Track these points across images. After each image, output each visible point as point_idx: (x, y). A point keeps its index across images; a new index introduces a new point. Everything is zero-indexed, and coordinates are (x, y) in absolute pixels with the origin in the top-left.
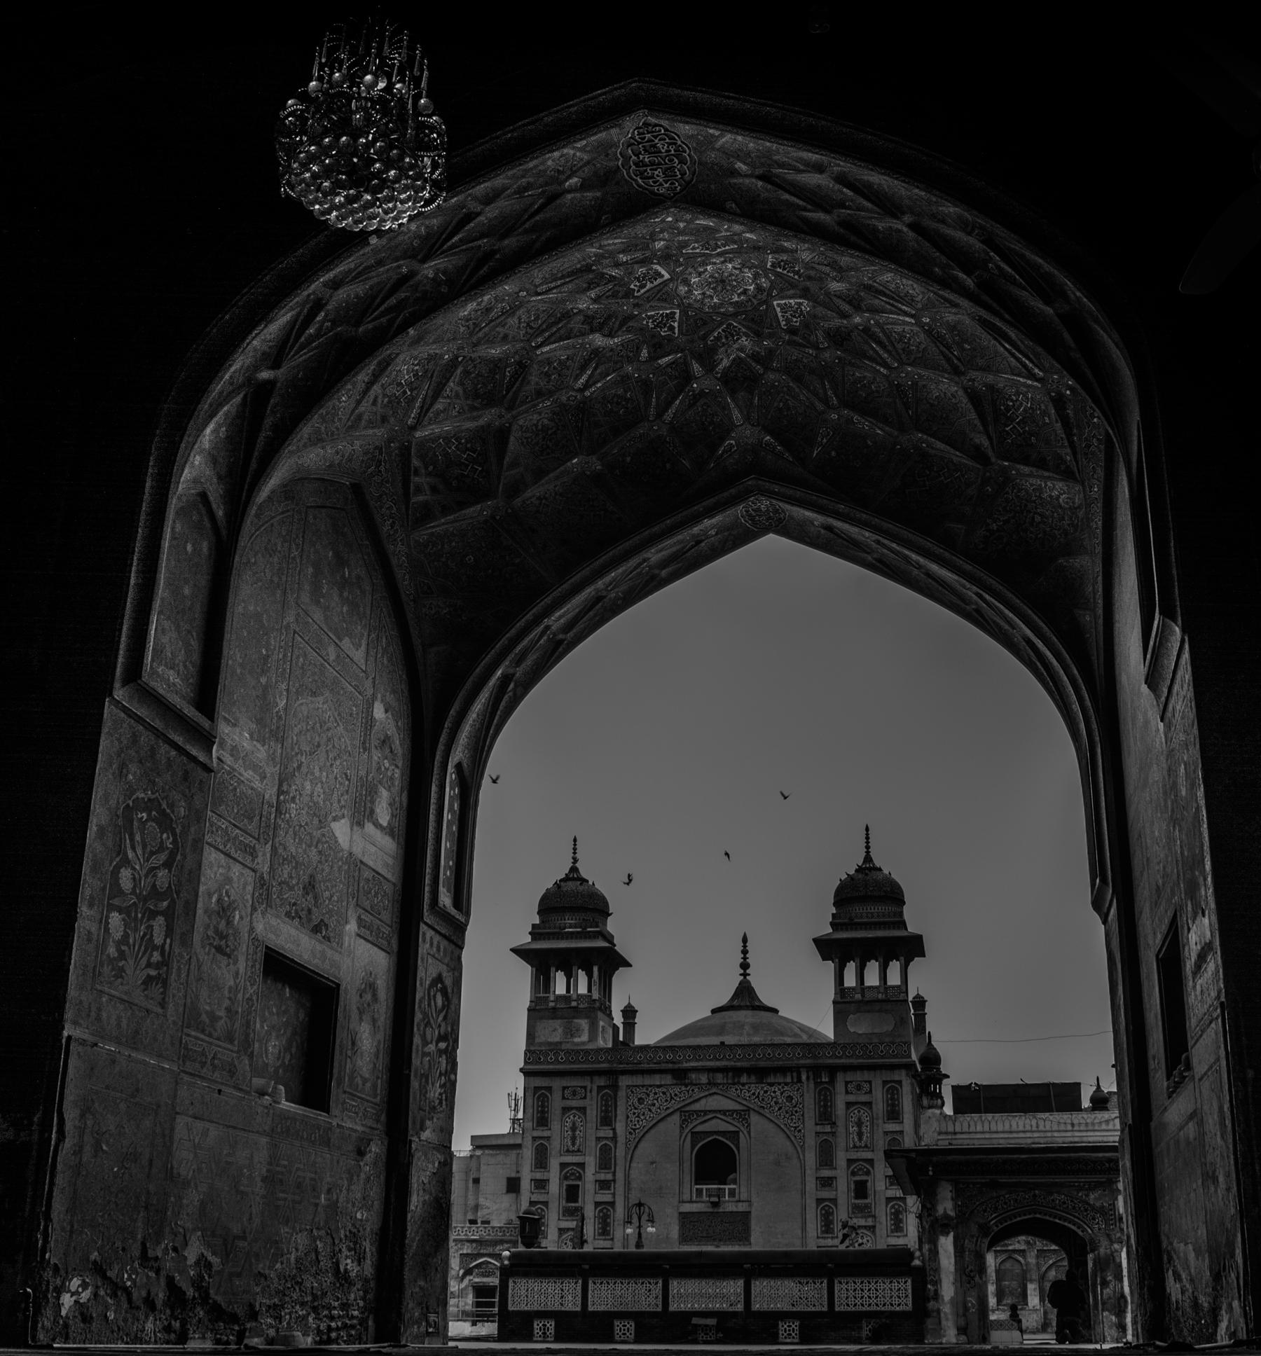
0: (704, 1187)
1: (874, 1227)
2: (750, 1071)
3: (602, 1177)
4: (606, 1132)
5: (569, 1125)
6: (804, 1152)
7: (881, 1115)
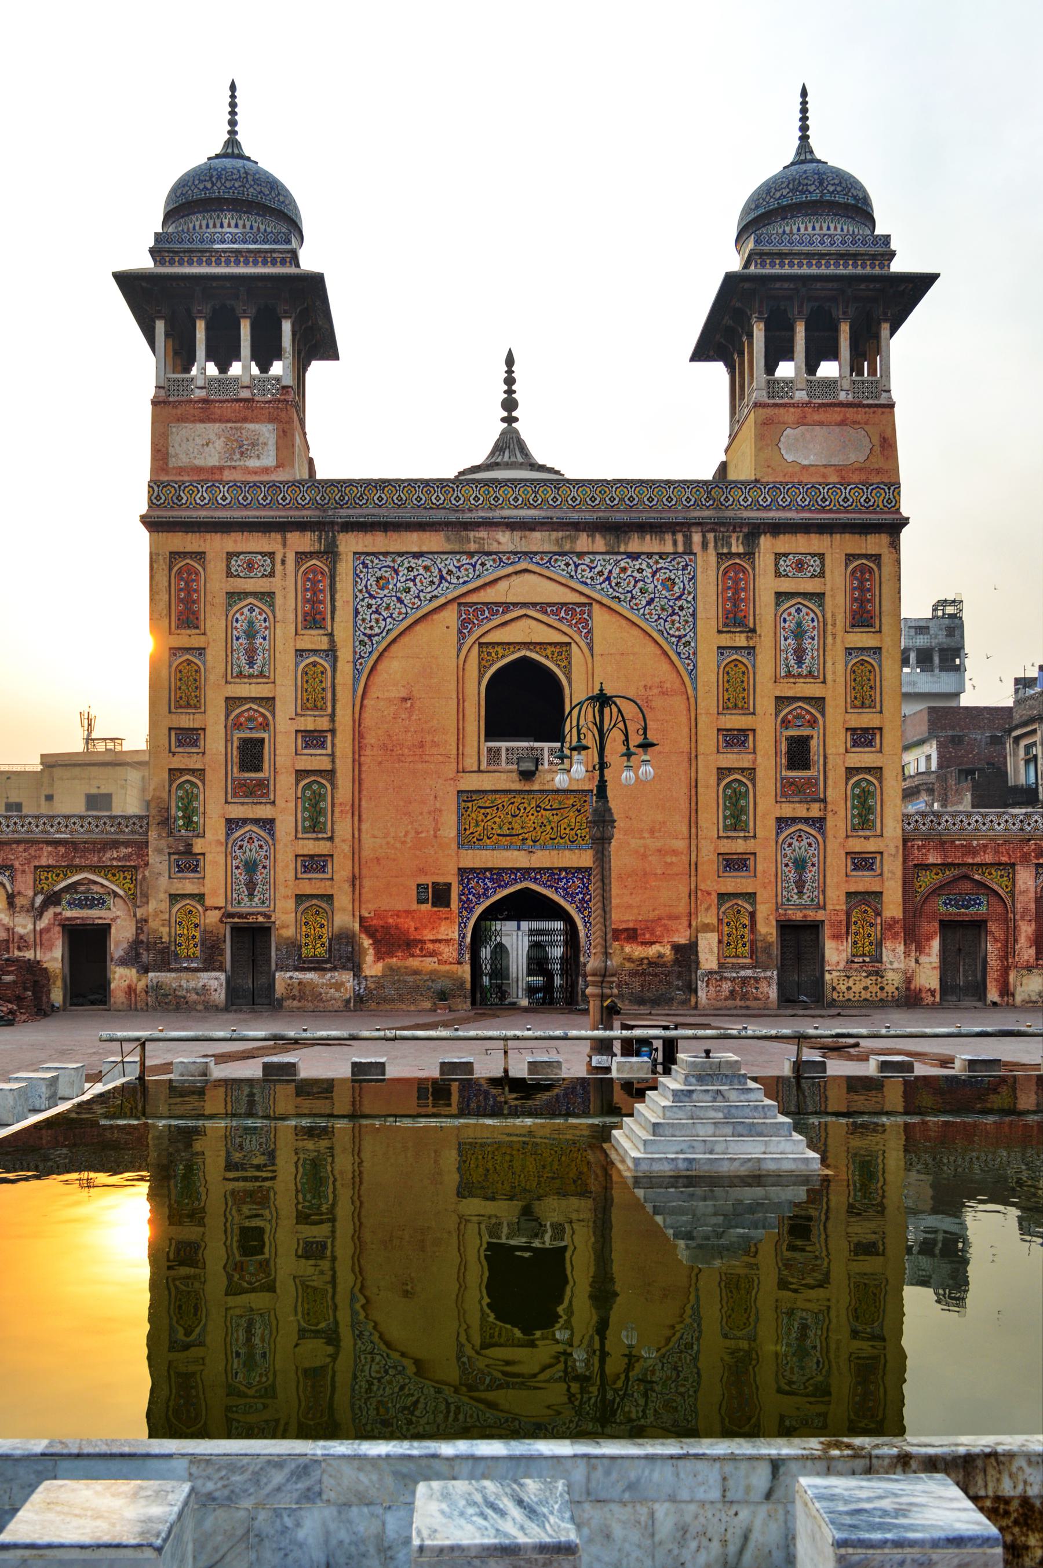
0: (503, 745)
1: (822, 820)
2: (594, 528)
3: (309, 723)
4: (316, 640)
5: (242, 625)
6: (694, 681)
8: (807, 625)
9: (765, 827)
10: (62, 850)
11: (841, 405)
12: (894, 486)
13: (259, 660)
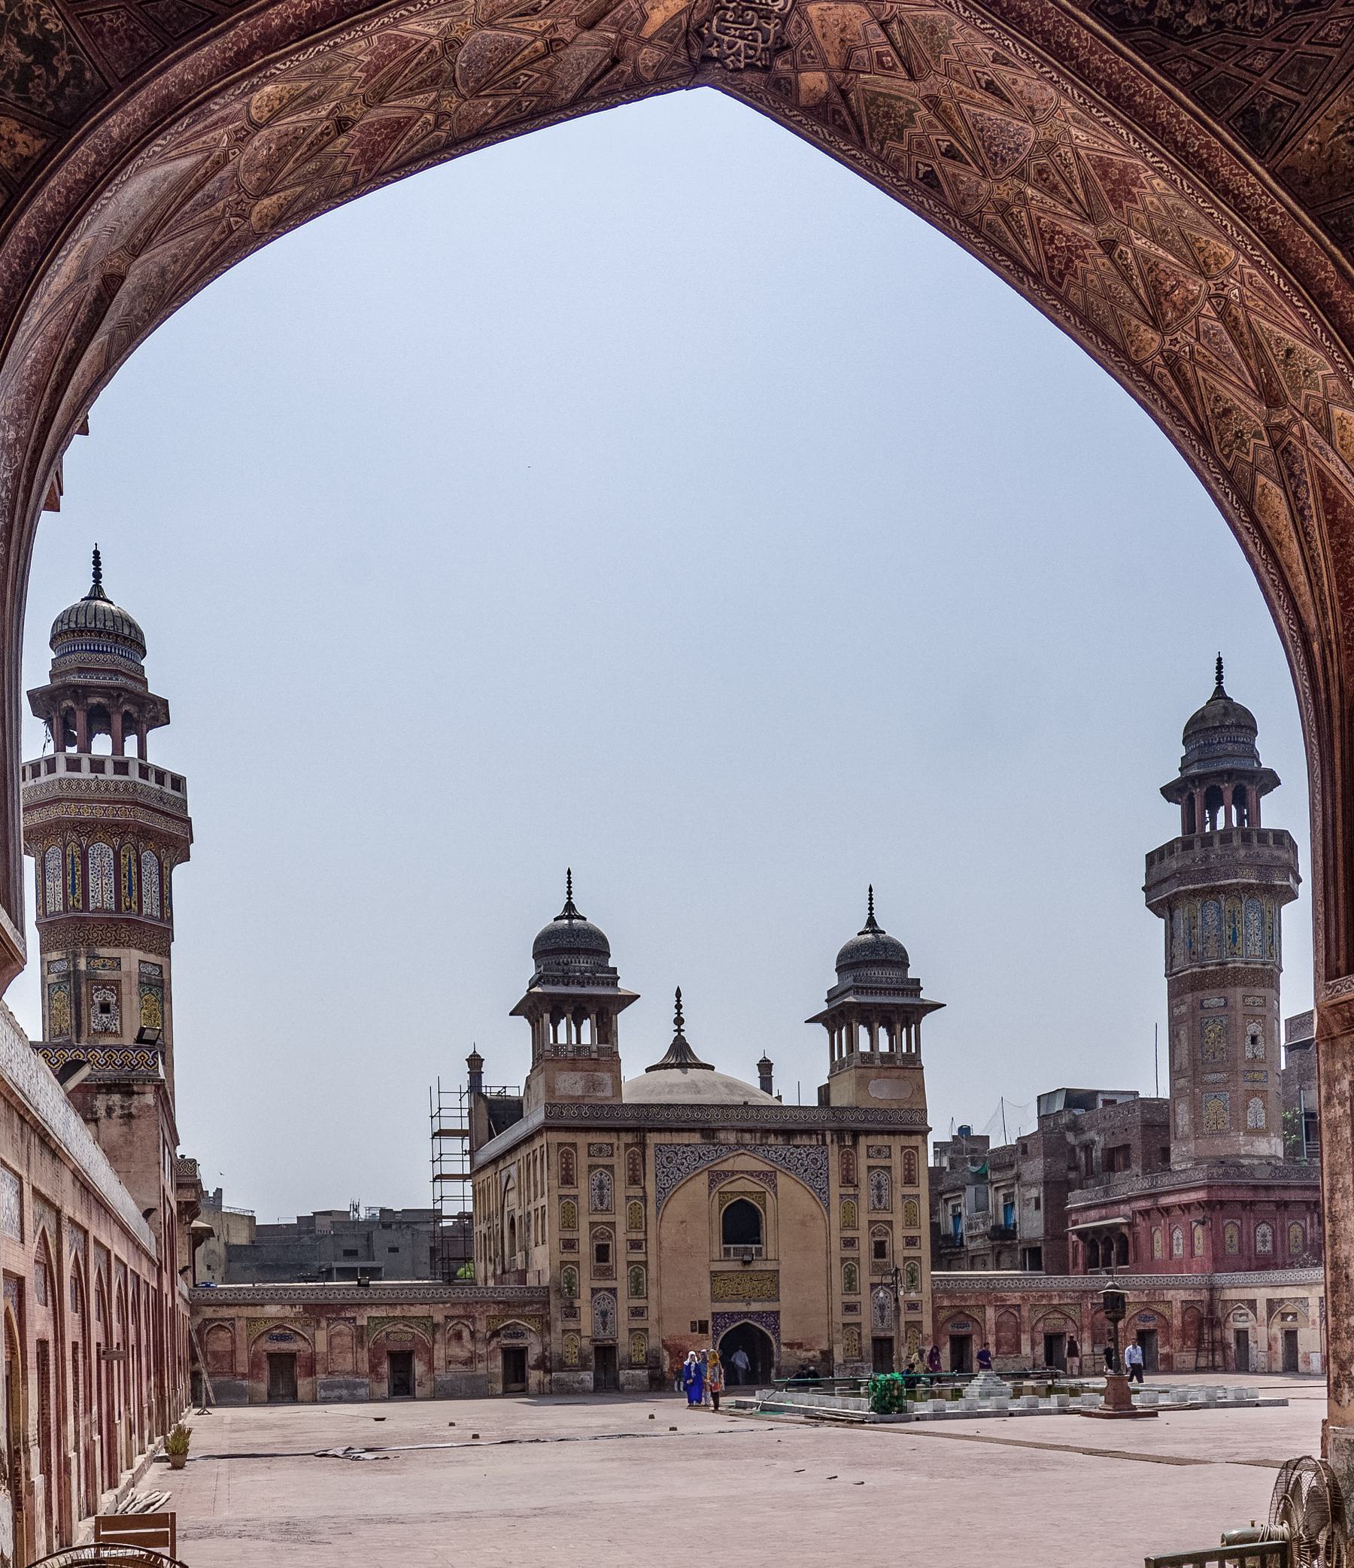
0: (732, 1246)
2: (777, 1132)
3: (634, 1236)
4: (635, 1191)
7: (899, 1179)
8: (883, 1183)
9: (865, 1289)
10: (501, 1306)
11: (898, 1068)
12: (926, 1111)
13: (606, 1202)
